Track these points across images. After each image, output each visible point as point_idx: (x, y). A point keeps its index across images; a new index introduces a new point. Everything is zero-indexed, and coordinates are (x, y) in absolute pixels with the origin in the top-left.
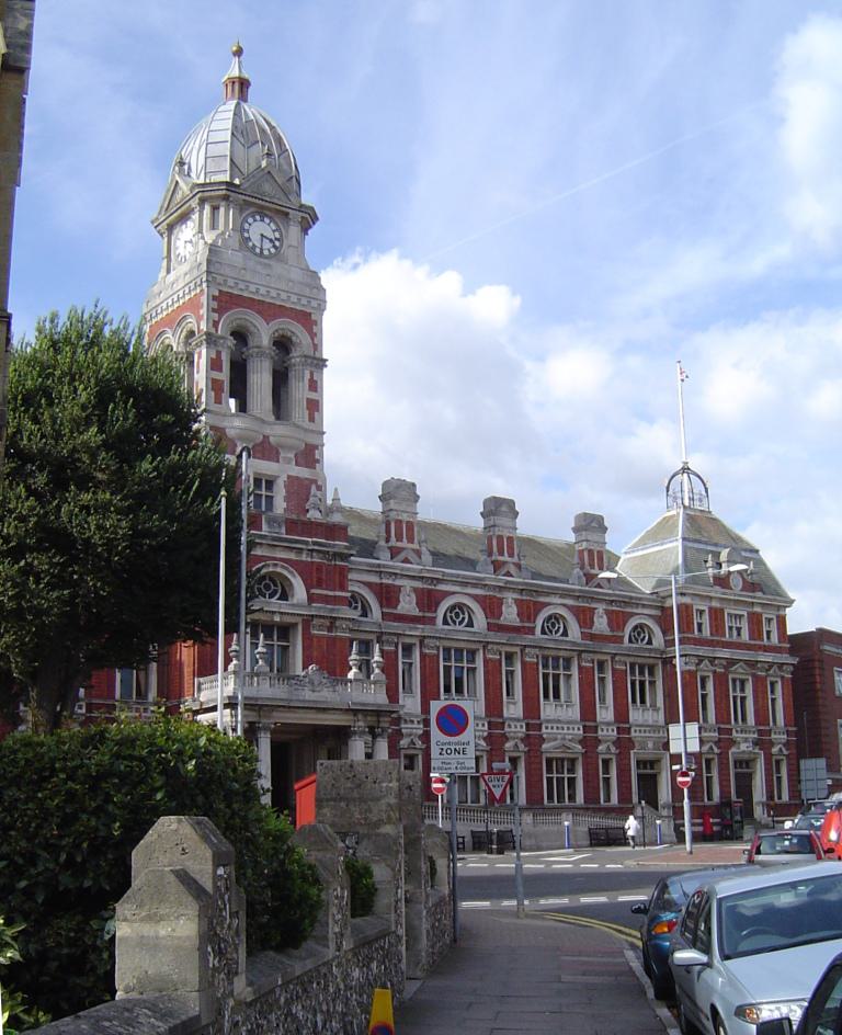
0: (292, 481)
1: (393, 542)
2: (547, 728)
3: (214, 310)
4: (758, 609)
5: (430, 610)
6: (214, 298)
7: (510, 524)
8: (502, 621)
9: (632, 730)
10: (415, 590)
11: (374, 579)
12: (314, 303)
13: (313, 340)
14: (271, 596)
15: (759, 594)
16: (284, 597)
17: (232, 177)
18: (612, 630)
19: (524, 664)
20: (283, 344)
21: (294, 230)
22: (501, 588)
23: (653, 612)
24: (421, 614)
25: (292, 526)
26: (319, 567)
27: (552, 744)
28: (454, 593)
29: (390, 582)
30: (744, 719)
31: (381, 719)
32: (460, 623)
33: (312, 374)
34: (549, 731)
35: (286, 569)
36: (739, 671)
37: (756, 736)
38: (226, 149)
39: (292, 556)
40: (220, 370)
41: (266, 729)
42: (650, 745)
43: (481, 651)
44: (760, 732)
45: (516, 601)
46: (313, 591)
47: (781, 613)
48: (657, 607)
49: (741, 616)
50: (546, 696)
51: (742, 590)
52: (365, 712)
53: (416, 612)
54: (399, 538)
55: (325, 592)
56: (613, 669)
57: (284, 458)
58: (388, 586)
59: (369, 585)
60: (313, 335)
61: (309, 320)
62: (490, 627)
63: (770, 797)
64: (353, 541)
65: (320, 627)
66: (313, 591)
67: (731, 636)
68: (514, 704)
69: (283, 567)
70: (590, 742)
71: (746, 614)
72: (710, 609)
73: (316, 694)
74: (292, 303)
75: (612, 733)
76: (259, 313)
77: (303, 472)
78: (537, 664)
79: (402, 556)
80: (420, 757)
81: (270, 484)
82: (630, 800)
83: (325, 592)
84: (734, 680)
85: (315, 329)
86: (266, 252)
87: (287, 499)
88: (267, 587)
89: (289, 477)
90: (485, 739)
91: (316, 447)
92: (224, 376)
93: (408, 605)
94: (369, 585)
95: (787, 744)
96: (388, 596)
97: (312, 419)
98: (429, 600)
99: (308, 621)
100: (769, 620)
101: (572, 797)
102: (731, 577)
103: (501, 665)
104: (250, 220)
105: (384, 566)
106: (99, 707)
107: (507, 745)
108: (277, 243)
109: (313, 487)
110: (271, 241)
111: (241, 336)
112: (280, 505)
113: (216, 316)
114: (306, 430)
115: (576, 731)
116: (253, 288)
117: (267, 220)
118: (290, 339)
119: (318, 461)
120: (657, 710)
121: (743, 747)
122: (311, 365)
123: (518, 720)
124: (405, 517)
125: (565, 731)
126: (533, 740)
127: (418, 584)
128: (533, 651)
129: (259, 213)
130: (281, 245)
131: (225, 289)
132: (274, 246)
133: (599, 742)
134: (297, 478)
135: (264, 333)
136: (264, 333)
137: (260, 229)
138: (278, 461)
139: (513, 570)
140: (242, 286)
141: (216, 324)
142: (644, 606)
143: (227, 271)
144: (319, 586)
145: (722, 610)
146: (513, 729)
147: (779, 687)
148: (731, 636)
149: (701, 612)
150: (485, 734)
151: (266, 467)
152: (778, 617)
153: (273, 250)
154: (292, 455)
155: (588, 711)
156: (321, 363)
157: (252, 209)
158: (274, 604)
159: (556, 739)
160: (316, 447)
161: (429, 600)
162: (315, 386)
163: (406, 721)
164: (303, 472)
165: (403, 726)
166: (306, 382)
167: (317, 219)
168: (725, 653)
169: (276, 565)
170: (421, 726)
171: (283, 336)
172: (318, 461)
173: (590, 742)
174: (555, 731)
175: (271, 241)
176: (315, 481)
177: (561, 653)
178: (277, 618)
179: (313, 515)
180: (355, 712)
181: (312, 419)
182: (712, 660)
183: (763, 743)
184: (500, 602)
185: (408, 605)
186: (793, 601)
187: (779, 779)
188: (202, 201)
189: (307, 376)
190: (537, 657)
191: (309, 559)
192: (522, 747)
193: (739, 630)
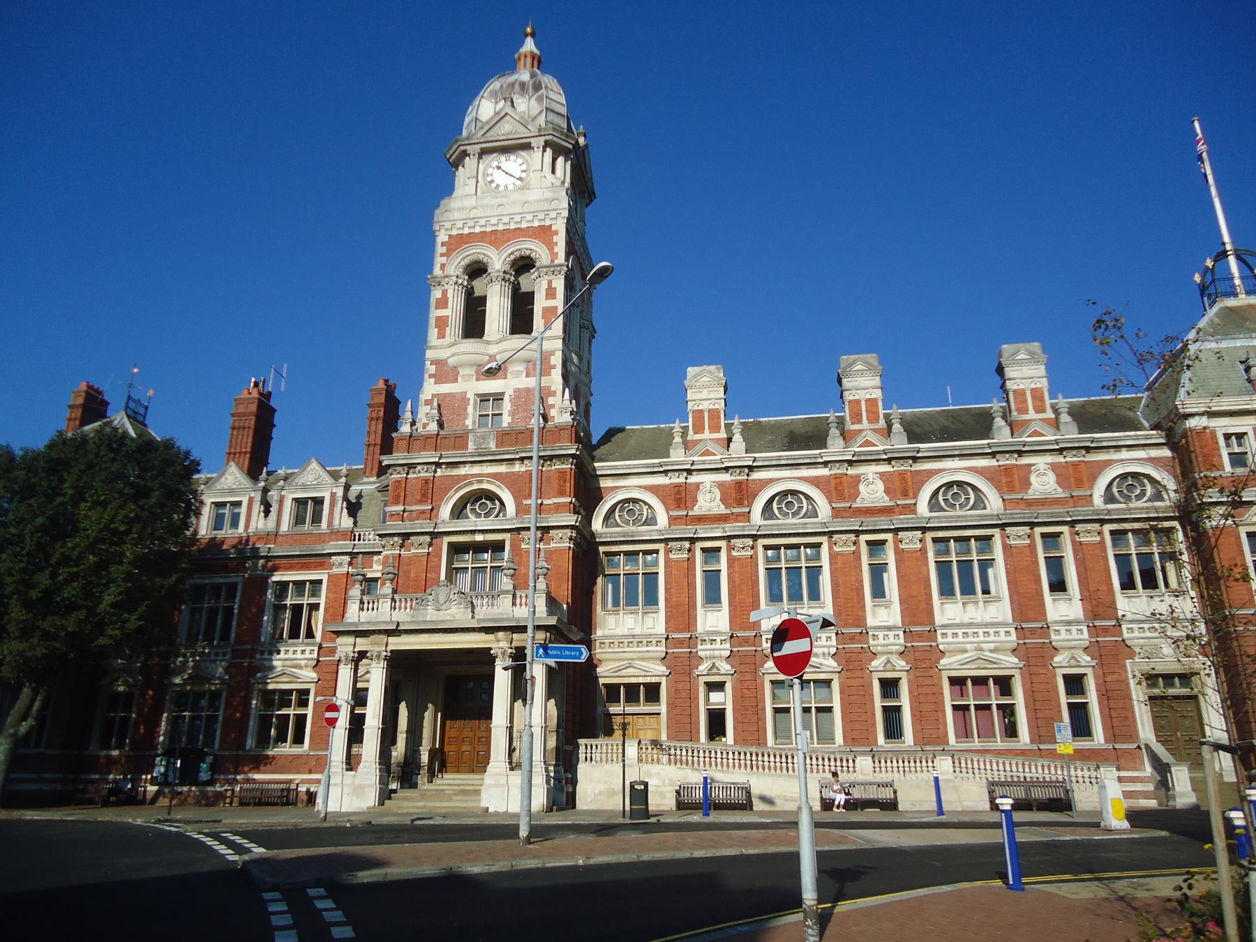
9: (1124, 627)
10: (721, 485)
27: (959, 657)
29: (682, 480)
33: (550, 282)
34: (950, 639)
35: (493, 483)
39: (502, 469)
50: (947, 591)
56: (1074, 543)
68: (888, 607)
69: (488, 482)
76: (491, 243)
87: (513, 414)
98: (740, 494)
101: (1011, 731)
107: (875, 663)
112: (506, 421)
115: (1003, 637)
125: (981, 638)
131: (454, 232)
135: (498, 261)
139: (871, 437)
143: (456, 215)
146: (881, 641)
150: (833, 650)
153: (518, 183)
159: (966, 651)
165: (699, 647)
169: (480, 482)
170: (728, 646)
174: (960, 639)
184: (857, 480)
189: (544, 285)
191: (523, 469)
192: (901, 664)
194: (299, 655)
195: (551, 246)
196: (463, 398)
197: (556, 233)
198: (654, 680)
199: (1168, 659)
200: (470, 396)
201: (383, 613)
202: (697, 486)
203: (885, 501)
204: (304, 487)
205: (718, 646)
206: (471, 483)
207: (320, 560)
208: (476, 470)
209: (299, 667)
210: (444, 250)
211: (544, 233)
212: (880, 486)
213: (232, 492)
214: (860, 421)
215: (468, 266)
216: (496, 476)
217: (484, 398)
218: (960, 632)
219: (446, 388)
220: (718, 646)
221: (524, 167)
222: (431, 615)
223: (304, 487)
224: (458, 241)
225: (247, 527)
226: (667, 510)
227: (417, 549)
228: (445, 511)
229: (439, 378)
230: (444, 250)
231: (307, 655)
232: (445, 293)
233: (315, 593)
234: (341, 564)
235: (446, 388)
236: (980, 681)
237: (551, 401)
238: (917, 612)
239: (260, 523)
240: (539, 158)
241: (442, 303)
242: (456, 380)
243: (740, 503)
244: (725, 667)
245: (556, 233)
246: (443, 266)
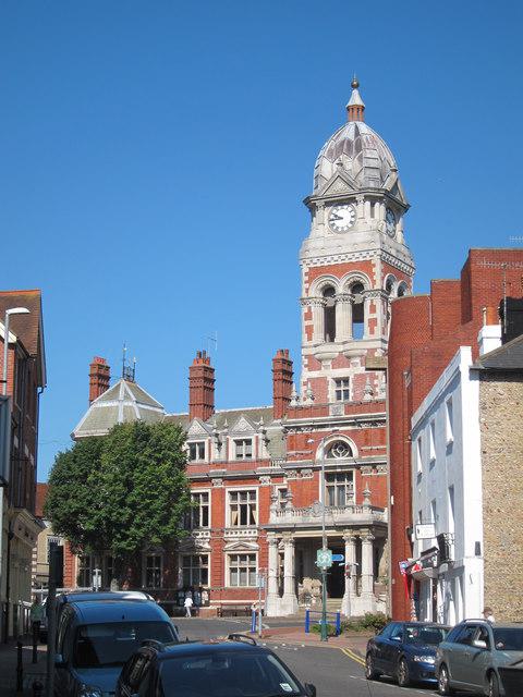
13: (372, 277)
39: (350, 428)
81: (346, 381)
89: (355, 375)
135: (341, 287)
136: (341, 287)
144: (366, 444)
180: (345, 527)
194: (248, 535)
195: (372, 275)
196: (323, 380)
197: (374, 265)
200: (329, 379)
201: (290, 518)
207: (254, 478)
210: (307, 278)
211: (367, 266)
213: (198, 436)
215: (322, 289)
216: (345, 432)
217: (338, 381)
219: (315, 374)
221: (353, 214)
222: (312, 520)
224: (315, 273)
225: (210, 457)
227: (308, 476)
228: (319, 454)
229: (311, 367)
230: (307, 278)
231: (252, 535)
232: (310, 308)
233: (253, 498)
235: (315, 374)
237: (376, 382)
239: (216, 456)
240: (364, 207)
241: (309, 316)
242: (320, 369)
245: (374, 265)
246: (307, 290)
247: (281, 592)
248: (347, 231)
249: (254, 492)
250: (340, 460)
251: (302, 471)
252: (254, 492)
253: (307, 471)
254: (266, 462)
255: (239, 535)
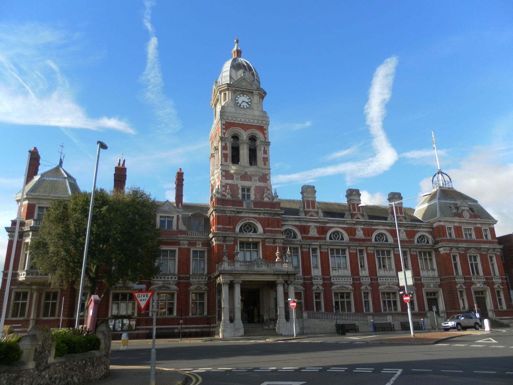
0: (258, 188)
1: (306, 209)
2: (380, 280)
3: (223, 129)
4: (479, 226)
5: (323, 234)
6: (224, 124)
7: (358, 199)
8: (356, 237)
9: (422, 279)
10: (316, 227)
11: (297, 223)
12: (264, 122)
13: (264, 136)
14: (249, 232)
15: (479, 219)
16: (255, 231)
17: (230, 82)
18: (408, 238)
19: (367, 254)
20: (253, 139)
21: (256, 99)
22: (354, 224)
23: (428, 230)
24: (319, 236)
25: (257, 204)
26: (268, 219)
28: (334, 227)
29: (305, 224)
30: (478, 273)
31: (290, 277)
32: (338, 239)
33: (264, 148)
34: (382, 281)
36: (472, 252)
37: (484, 280)
38: (228, 73)
39: (257, 216)
40: (227, 150)
41: (238, 283)
42: (432, 286)
43: (348, 250)
44: (487, 279)
45: (362, 229)
46: (266, 229)
47: (491, 226)
48: (429, 228)
49: (471, 229)
51: (470, 218)
52: (283, 275)
53: (317, 235)
54: (308, 207)
55: (271, 229)
56: (410, 254)
57: (254, 179)
58: (304, 226)
59: (296, 226)
60: (264, 134)
61: (262, 129)
62: (351, 240)
63: (496, 307)
64: (282, 209)
65: (269, 242)
66: (266, 229)
67: (467, 237)
68: (365, 270)
70: (357, 285)
71: (473, 228)
72: (455, 227)
73: (260, 268)
74: (255, 123)
75: (368, 281)
76: (242, 128)
77: (262, 184)
78: (374, 253)
79: (310, 214)
80: (322, 294)
81: (249, 190)
82: (424, 310)
83: (271, 229)
84: (470, 257)
85: (265, 132)
86: (245, 107)
87: (255, 195)
88: (248, 228)
89: (256, 186)
90: (351, 285)
91: (267, 175)
92: (229, 152)
93: (313, 233)
94: (296, 226)
95: (502, 284)
96: (304, 230)
97: (265, 164)
98: (323, 230)
99: (264, 241)
100: (486, 230)
102: (464, 213)
103: (357, 254)
104: (239, 96)
105: (301, 218)
106: (183, 278)
107: (362, 287)
108: (250, 103)
109: (266, 191)
110: (247, 103)
111: (236, 137)
112: (253, 197)
113: (224, 131)
114: (263, 169)
115: (394, 281)
116: (239, 119)
117: (245, 96)
118: (255, 136)
119: (268, 180)
120: (433, 269)
121: (478, 285)
122: (264, 144)
123: (366, 277)
124: (310, 199)
125: (389, 281)
126: (327, 284)
127: (318, 225)
128: (371, 248)
129: (241, 93)
130: (251, 104)
131: (228, 121)
132: (249, 104)
133: (362, 285)
134: (259, 186)
135: (244, 135)
136: (244, 135)
137: (242, 99)
138: (251, 181)
139: (360, 216)
140: (234, 119)
141: (224, 134)
142: (423, 228)
143: (228, 114)
144: (268, 226)
145: (460, 227)
146: (364, 281)
147: (494, 258)
148: (467, 237)
149: (450, 228)
150: (351, 283)
151: (246, 184)
152: (490, 228)
153: (248, 106)
154: (257, 178)
155: (355, 271)
156: (268, 144)
157: (239, 92)
158: (251, 234)
159: (385, 284)
160: (267, 175)
161: (323, 230)
162: (265, 152)
163: (315, 279)
164: (262, 184)
166: (262, 151)
167: (265, 93)
168: (464, 245)
169: (249, 220)
170: (322, 281)
171: (252, 136)
172: (268, 180)
173: (357, 285)
174: (384, 281)
175: (247, 103)
176: (267, 188)
177: (385, 249)
178: (251, 240)
179: (266, 199)
181: (265, 164)
182: (457, 248)
183: (489, 283)
184: (355, 230)
185: (313, 233)
186: (497, 221)
187: (500, 300)
188: (220, 93)
189: (263, 149)
190: (374, 251)
192: (369, 288)
193: (470, 235)
194: (170, 279)
198: (348, 291)
199: (432, 288)
200: (239, 186)
202: (309, 226)
203: (363, 237)
204: (165, 212)
205: (319, 280)
206: (246, 220)
208: (247, 215)
209: (170, 284)
212: (362, 232)
214: (355, 211)
218: (384, 279)
220: (319, 280)
223: (165, 212)
226: (301, 234)
231: (173, 279)
234: (184, 245)
236: (388, 294)
238: (373, 272)
243: (323, 234)
244: (321, 288)
247: (232, 320)
248: (245, 109)
249: (174, 251)
250: (250, 236)
251: (227, 239)
252: (174, 251)
253: (230, 239)
254: (184, 233)
255: (163, 279)
